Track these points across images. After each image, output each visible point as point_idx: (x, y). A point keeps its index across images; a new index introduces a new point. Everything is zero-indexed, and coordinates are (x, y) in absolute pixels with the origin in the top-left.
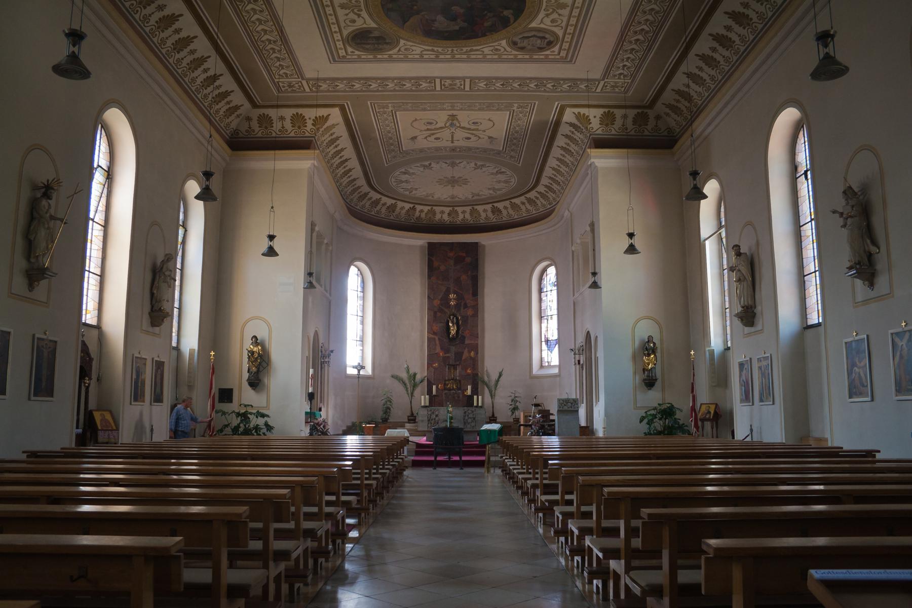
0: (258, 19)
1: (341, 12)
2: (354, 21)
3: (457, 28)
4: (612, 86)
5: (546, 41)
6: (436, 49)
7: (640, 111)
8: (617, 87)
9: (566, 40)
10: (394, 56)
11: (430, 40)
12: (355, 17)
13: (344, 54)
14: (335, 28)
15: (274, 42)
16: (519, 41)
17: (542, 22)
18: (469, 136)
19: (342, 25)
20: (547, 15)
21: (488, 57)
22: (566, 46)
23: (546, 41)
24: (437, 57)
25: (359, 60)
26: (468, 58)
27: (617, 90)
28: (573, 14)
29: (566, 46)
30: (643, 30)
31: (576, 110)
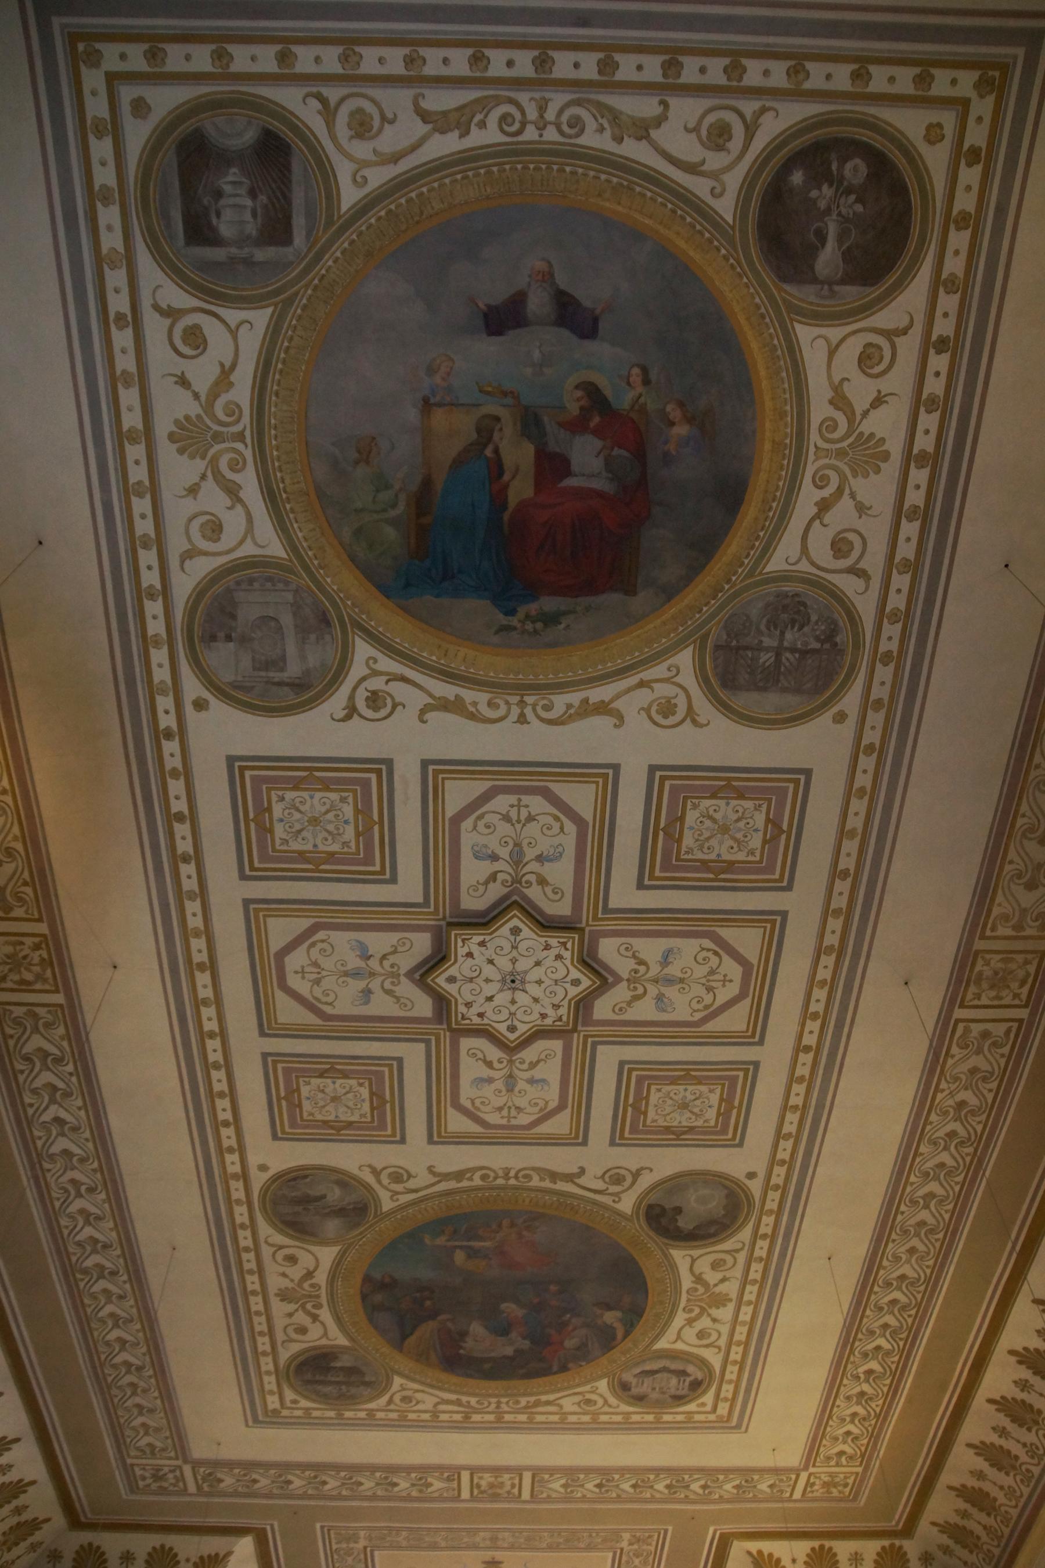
0: (112, 1315)
1: (279, 1308)
2: (302, 1330)
3: (509, 1351)
4: (825, 1484)
5: (690, 1381)
6: (464, 1399)
7: (886, 1543)
8: (835, 1485)
9: (728, 1376)
10: (380, 1415)
11: (454, 1379)
12: (306, 1321)
13: (277, 1405)
14: (263, 1343)
15: (139, 1369)
16: (634, 1381)
17: (679, 1337)
19: (280, 1336)
20: (690, 1322)
21: (573, 1418)
22: (728, 1390)
23: (690, 1381)
24: (467, 1417)
25: (307, 1421)
26: (531, 1421)
27: (835, 1492)
28: (741, 1318)
29: (728, 1390)
30: (878, 1348)
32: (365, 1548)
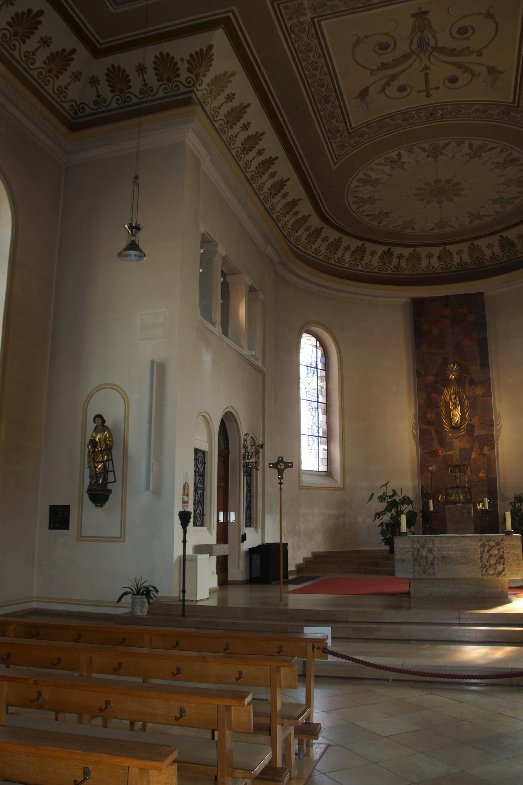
18: (454, 71)
32: (312, 19)
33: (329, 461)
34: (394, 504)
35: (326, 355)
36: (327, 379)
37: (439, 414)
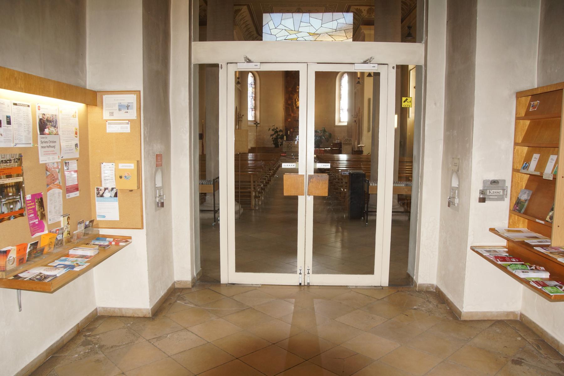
31: (356, 7)
33: (255, 117)
34: (277, 132)
35: (255, 80)
36: (255, 88)
37: (292, 102)
